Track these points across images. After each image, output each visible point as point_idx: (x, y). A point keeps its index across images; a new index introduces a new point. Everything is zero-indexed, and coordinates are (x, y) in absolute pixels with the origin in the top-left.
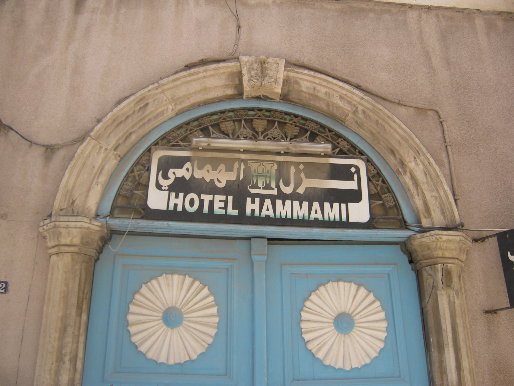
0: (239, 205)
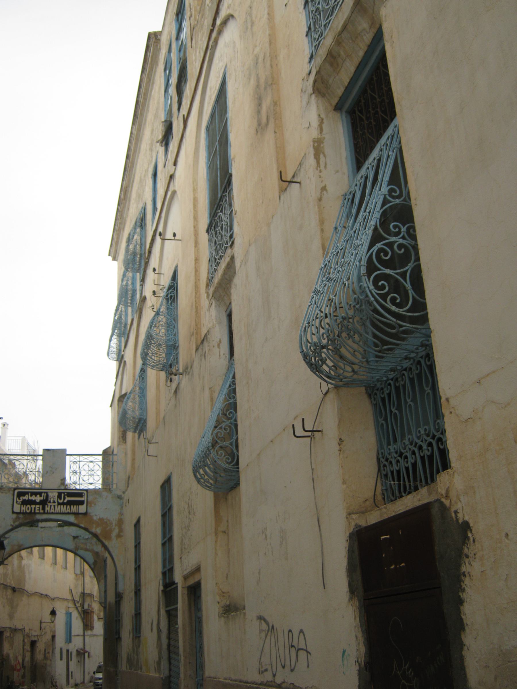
0: (44, 509)
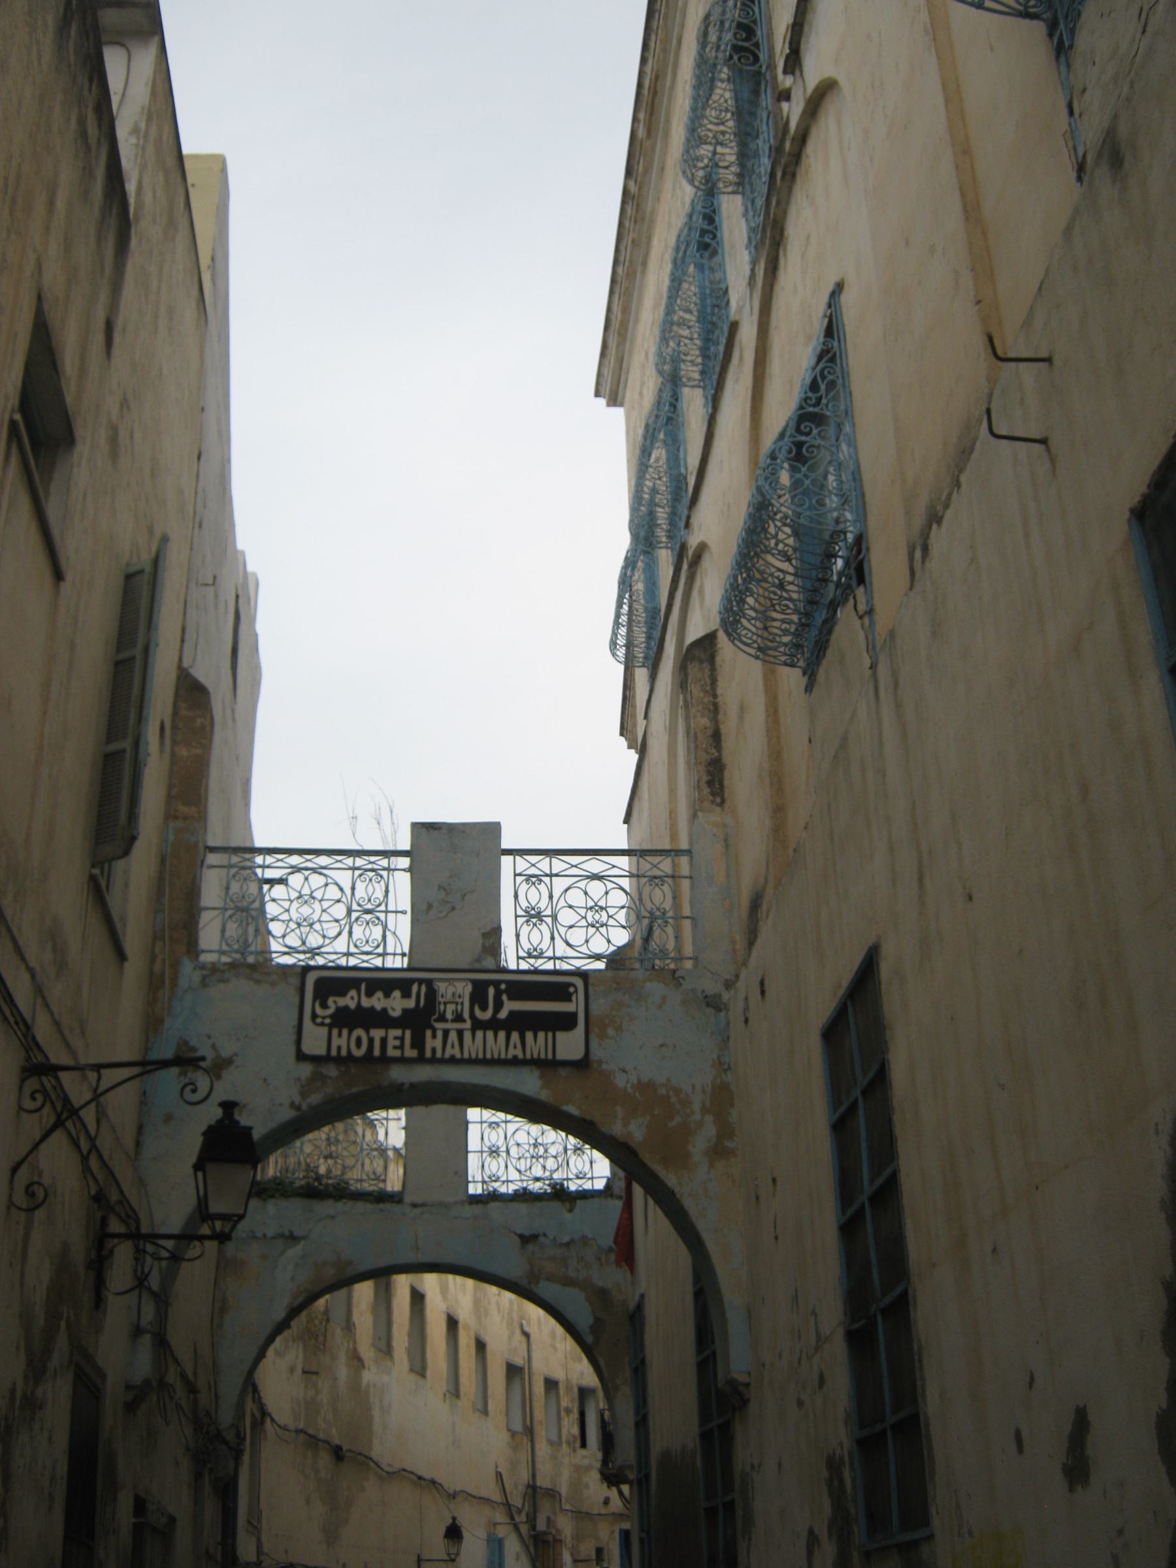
0: (418, 1043)
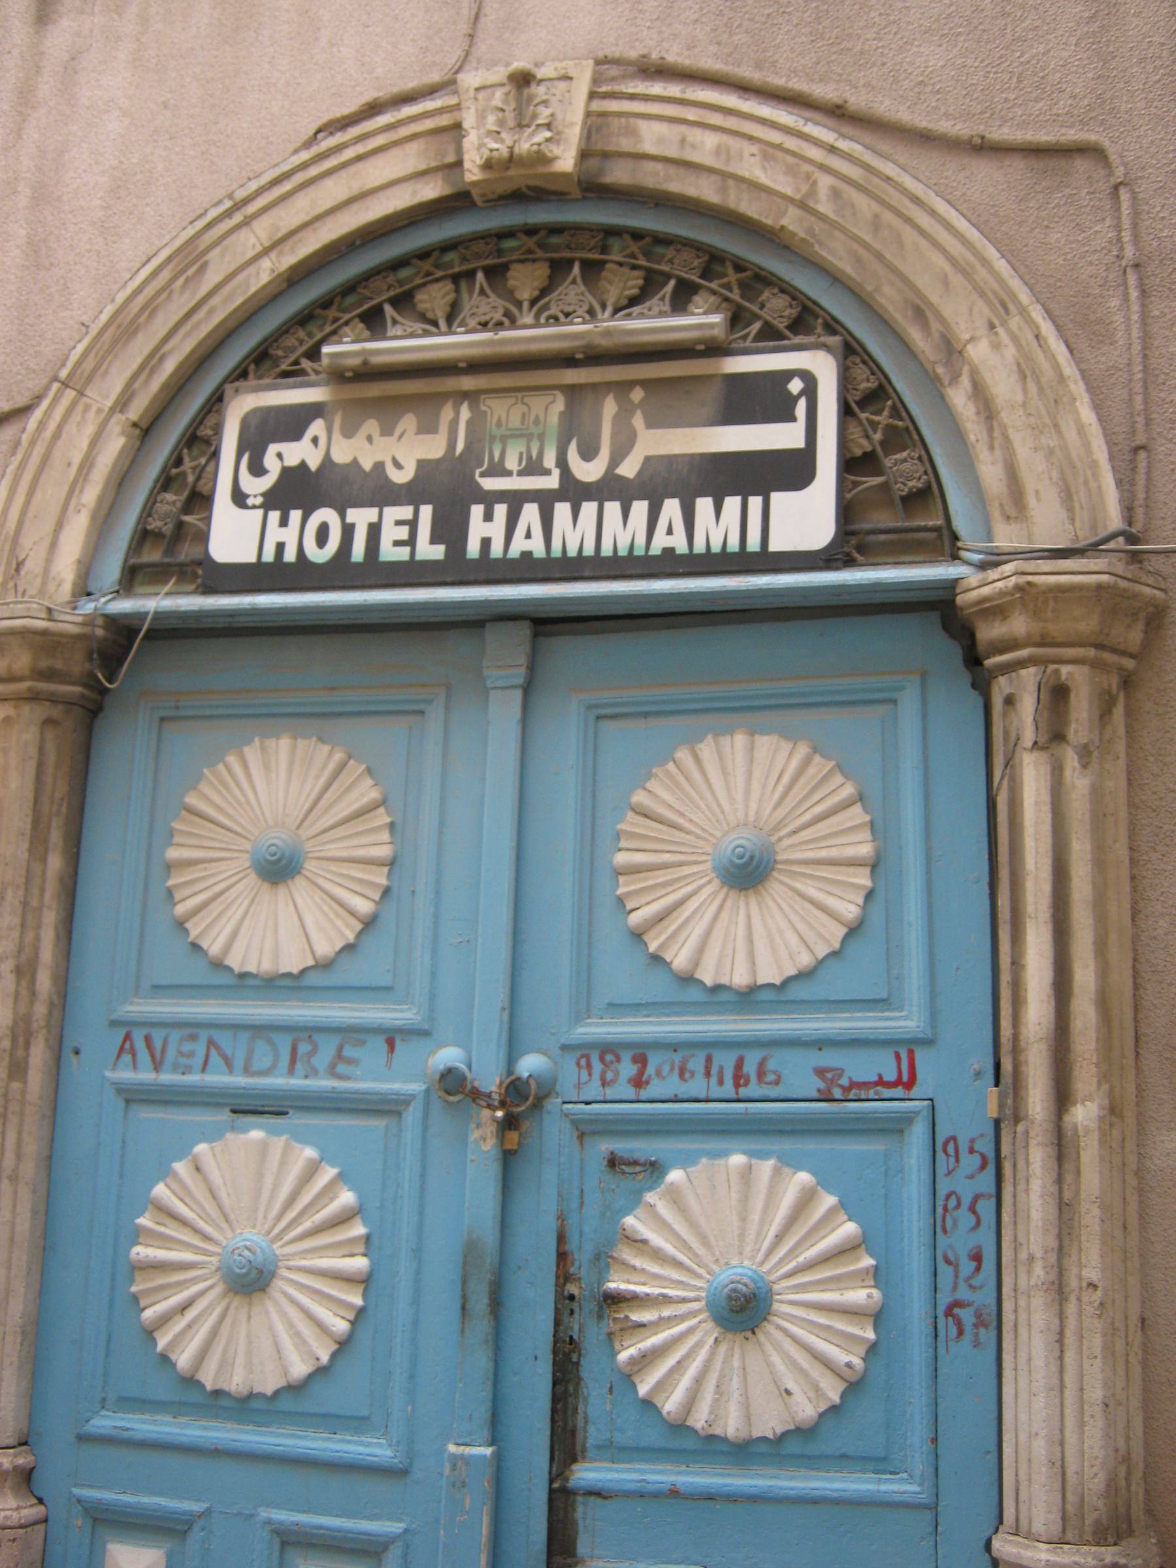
0: (450, 529)
